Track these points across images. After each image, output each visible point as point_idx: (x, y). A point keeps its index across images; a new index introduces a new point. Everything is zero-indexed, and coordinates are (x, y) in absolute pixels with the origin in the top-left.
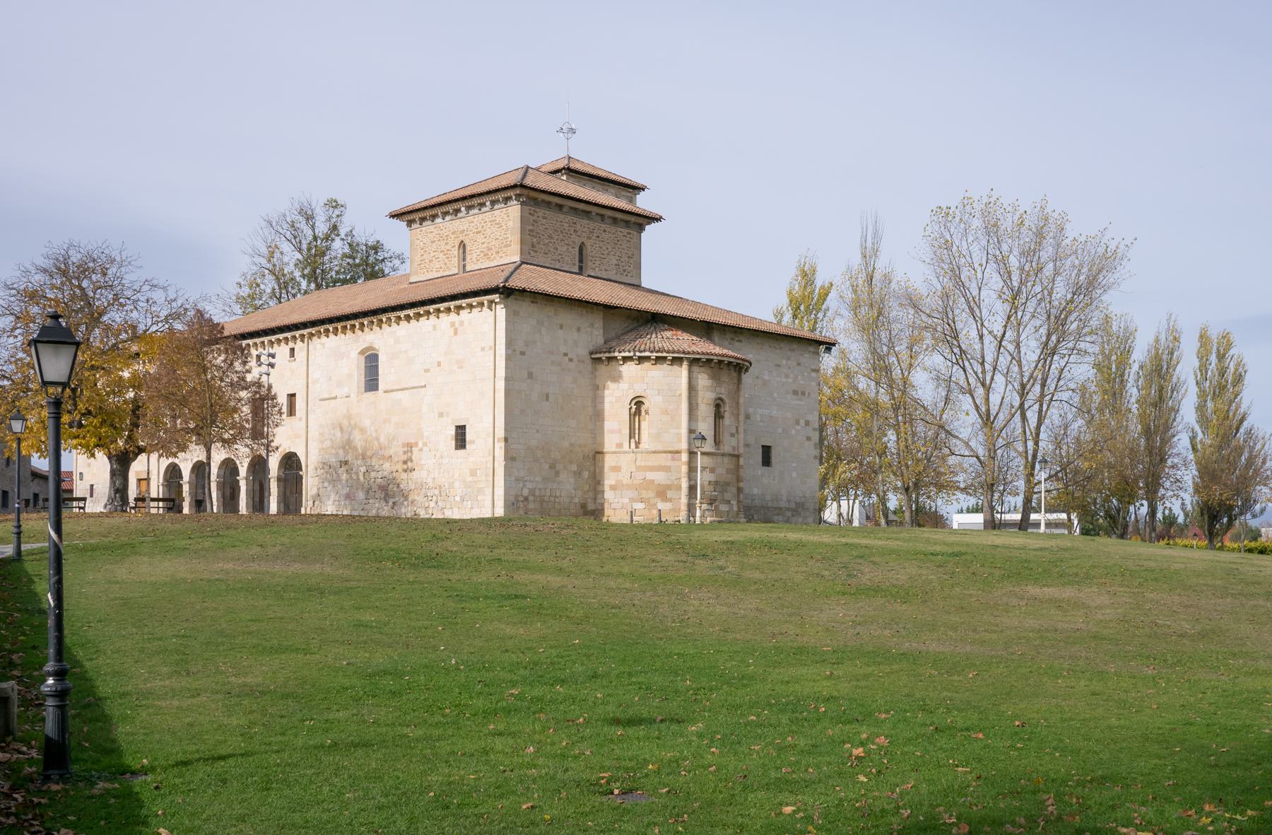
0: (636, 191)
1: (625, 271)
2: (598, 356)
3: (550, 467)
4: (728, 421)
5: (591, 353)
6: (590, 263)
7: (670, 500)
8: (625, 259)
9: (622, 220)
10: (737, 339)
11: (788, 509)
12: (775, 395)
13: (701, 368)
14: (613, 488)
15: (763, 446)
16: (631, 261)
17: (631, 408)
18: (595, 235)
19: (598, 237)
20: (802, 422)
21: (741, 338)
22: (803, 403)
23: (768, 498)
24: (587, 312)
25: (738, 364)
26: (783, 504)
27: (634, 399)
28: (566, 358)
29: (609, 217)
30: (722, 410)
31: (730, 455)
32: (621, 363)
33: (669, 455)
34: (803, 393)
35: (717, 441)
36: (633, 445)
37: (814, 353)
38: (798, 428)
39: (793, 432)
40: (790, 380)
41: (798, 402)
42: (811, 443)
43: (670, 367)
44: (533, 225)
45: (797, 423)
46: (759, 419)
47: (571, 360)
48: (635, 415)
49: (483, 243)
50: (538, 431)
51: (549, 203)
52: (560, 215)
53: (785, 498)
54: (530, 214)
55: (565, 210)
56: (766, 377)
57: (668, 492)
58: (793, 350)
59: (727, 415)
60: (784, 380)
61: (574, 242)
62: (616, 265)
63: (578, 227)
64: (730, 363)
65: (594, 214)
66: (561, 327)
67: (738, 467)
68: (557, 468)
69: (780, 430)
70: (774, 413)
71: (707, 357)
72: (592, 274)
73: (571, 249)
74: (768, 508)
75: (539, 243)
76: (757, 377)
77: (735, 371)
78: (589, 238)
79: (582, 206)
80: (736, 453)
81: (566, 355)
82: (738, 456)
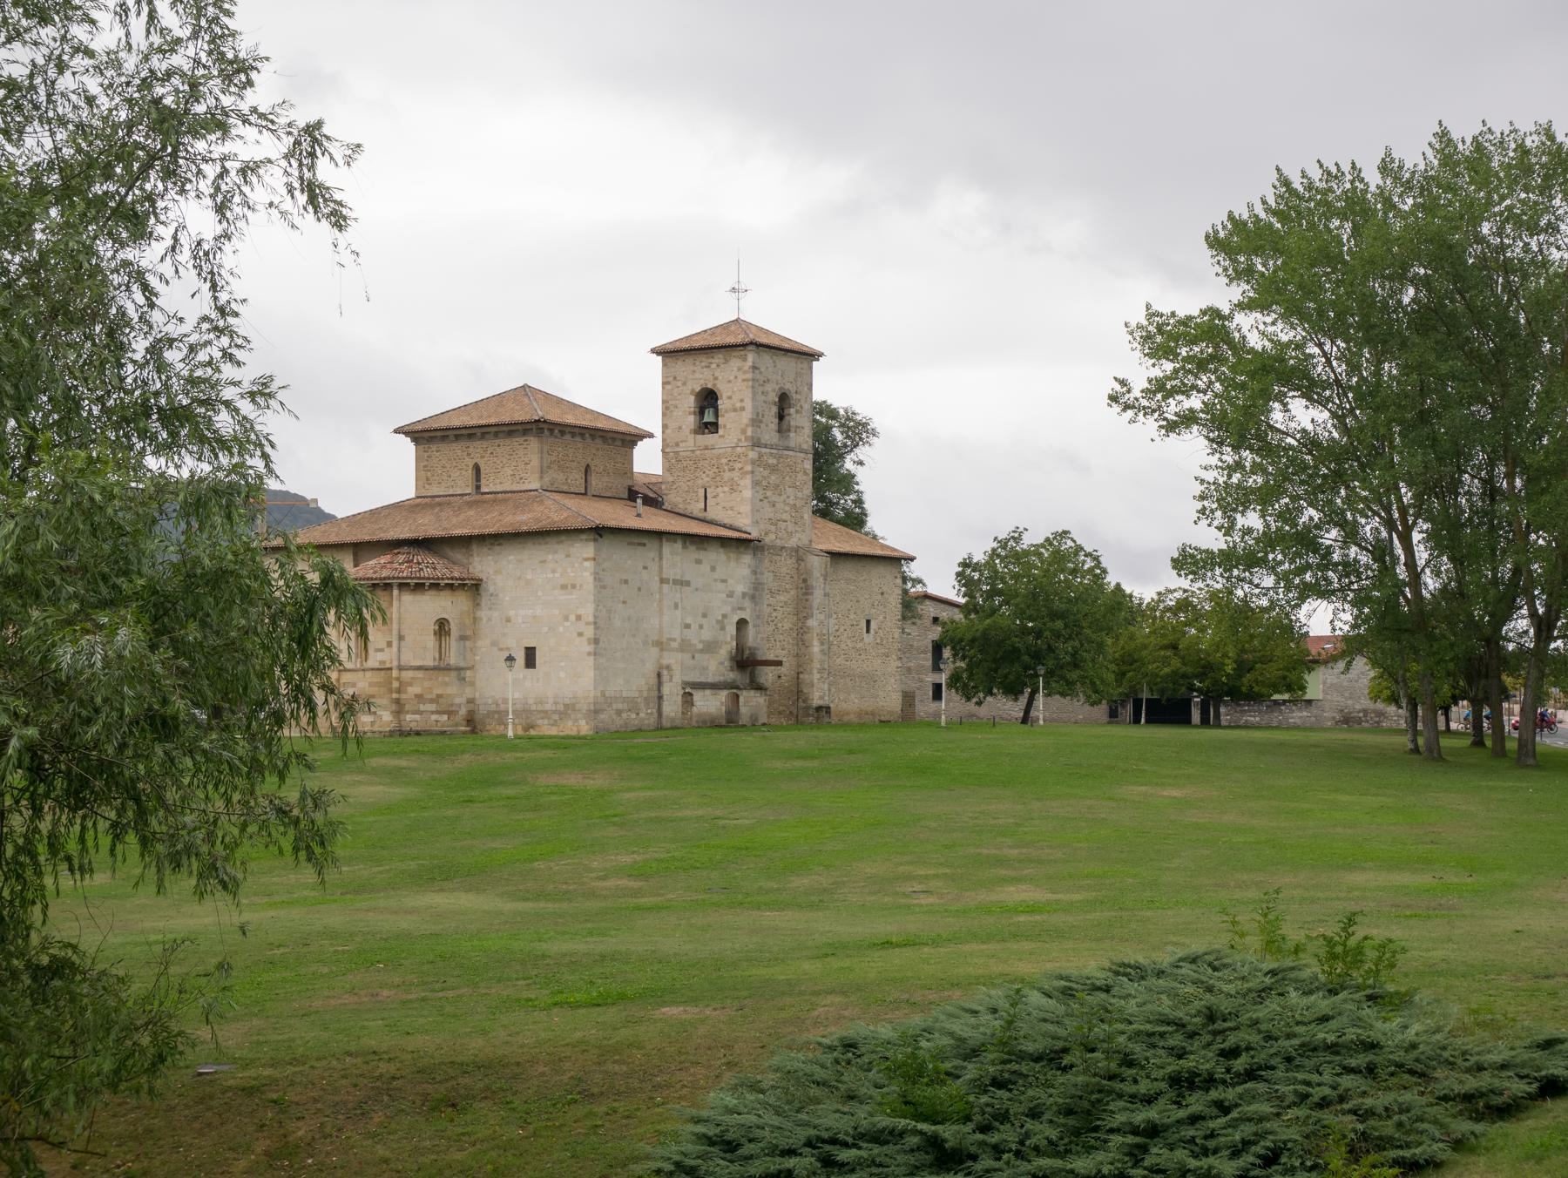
8: (521, 466)
11: (554, 712)
12: (540, 593)
20: (572, 618)
23: (531, 701)
26: (548, 707)
34: (574, 586)
38: (568, 624)
39: (561, 629)
42: (584, 639)
45: (566, 618)
51: (432, 437)
53: (551, 701)
56: (529, 577)
69: (546, 629)
70: (538, 611)
74: (531, 712)
76: (520, 578)
78: (482, 457)
79: (464, 432)
80: (388, 665)
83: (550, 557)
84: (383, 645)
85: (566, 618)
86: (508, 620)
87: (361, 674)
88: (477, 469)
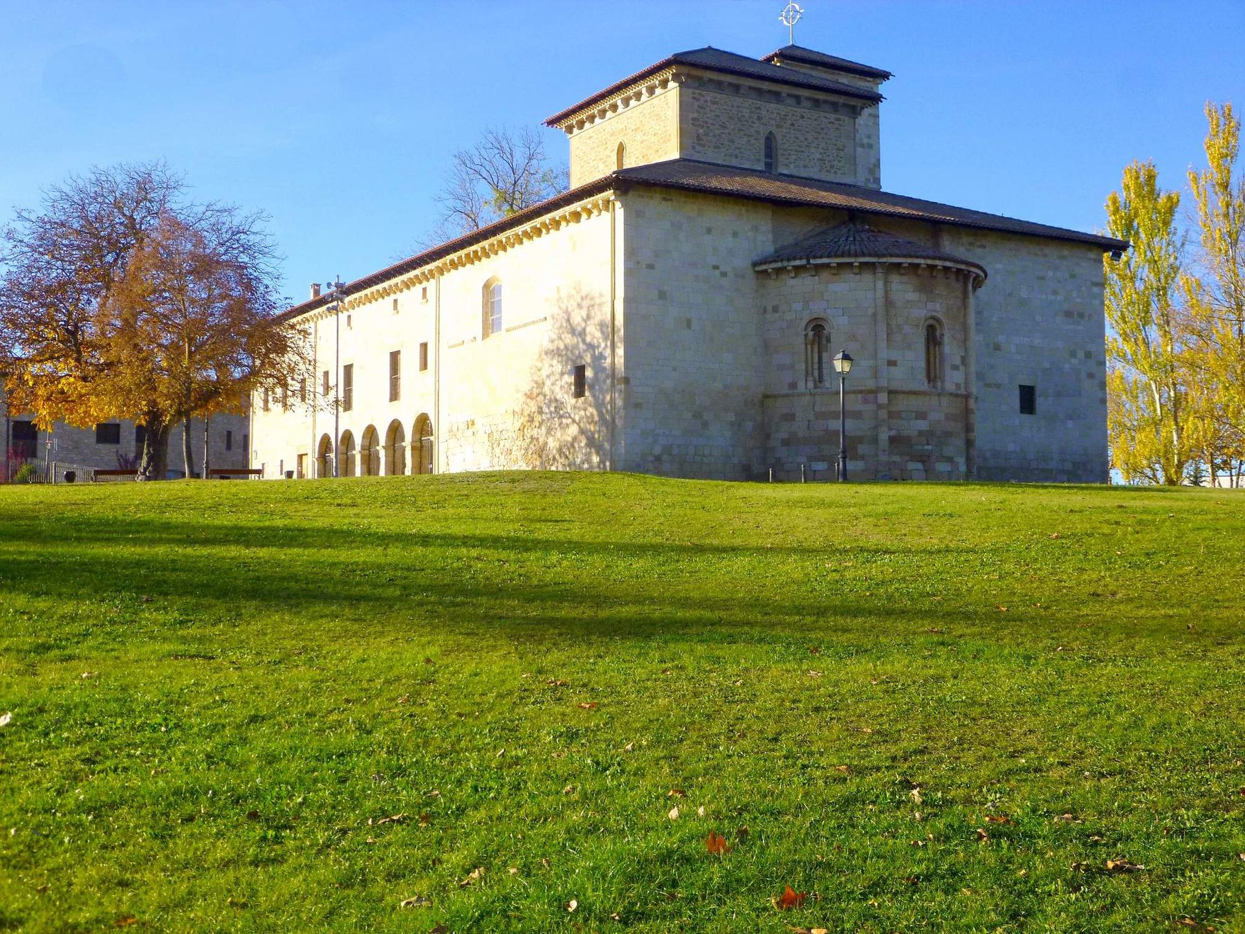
0: (878, 81)
1: (832, 167)
2: (764, 267)
3: (694, 416)
4: (950, 348)
5: (755, 264)
6: (781, 159)
7: (863, 458)
9: (825, 102)
10: (978, 244)
13: (905, 278)
14: (786, 443)
15: (1020, 386)
16: (842, 154)
17: (806, 335)
18: (789, 122)
19: (793, 125)
20: (1081, 354)
21: (984, 242)
22: (1082, 328)
24: (747, 211)
25: (959, 270)
27: (810, 321)
28: (717, 272)
29: (808, 99)
30: (938, 334)
31: (951, 394)
32: (793, 275)
33: (860, 396)
35: (932, 375)
36: (811, 385)
37: (1095, 260)
38: (1073, 361)
40: (1059, 298)
41: (1072, 327)
43: (858, 277)
44: (698, 112)
45: (1073, 354)
46: (1013, 350)
47: (724, 274)
48: (812, 344)
49: (642, 142)
50: (675, 369)
52: (737, 98)
54: (694, 98)
55: (742, 91)
56: (1024, 294)
57: (859, 446)
58: (1063, 258)
59: (946, 339)
60: (1051, 297)
61: (758, 132)
62: (820, 160)
63: (764, 113)
64: (946, 269)
65: (784, 95)
66: (709, 231)
67: (967, 411)
68: (705, 417)
71: (910, 260)
72: (785, 172)
73: (753, 141)
75: (707, 135)
76: (1010, 295)
77: (958, 280)
78: (778, 126)
81: (716, 267)
82: (967, 397)
83: (1050, 274)
84: (958, 361)
85: (1073, 354)
86: (997, 348)
87: (934, 401)
88: (770, 139)
